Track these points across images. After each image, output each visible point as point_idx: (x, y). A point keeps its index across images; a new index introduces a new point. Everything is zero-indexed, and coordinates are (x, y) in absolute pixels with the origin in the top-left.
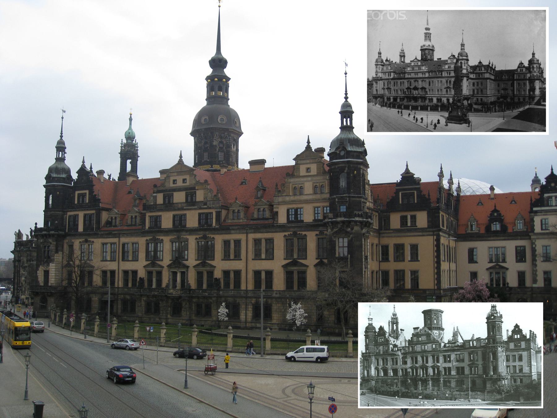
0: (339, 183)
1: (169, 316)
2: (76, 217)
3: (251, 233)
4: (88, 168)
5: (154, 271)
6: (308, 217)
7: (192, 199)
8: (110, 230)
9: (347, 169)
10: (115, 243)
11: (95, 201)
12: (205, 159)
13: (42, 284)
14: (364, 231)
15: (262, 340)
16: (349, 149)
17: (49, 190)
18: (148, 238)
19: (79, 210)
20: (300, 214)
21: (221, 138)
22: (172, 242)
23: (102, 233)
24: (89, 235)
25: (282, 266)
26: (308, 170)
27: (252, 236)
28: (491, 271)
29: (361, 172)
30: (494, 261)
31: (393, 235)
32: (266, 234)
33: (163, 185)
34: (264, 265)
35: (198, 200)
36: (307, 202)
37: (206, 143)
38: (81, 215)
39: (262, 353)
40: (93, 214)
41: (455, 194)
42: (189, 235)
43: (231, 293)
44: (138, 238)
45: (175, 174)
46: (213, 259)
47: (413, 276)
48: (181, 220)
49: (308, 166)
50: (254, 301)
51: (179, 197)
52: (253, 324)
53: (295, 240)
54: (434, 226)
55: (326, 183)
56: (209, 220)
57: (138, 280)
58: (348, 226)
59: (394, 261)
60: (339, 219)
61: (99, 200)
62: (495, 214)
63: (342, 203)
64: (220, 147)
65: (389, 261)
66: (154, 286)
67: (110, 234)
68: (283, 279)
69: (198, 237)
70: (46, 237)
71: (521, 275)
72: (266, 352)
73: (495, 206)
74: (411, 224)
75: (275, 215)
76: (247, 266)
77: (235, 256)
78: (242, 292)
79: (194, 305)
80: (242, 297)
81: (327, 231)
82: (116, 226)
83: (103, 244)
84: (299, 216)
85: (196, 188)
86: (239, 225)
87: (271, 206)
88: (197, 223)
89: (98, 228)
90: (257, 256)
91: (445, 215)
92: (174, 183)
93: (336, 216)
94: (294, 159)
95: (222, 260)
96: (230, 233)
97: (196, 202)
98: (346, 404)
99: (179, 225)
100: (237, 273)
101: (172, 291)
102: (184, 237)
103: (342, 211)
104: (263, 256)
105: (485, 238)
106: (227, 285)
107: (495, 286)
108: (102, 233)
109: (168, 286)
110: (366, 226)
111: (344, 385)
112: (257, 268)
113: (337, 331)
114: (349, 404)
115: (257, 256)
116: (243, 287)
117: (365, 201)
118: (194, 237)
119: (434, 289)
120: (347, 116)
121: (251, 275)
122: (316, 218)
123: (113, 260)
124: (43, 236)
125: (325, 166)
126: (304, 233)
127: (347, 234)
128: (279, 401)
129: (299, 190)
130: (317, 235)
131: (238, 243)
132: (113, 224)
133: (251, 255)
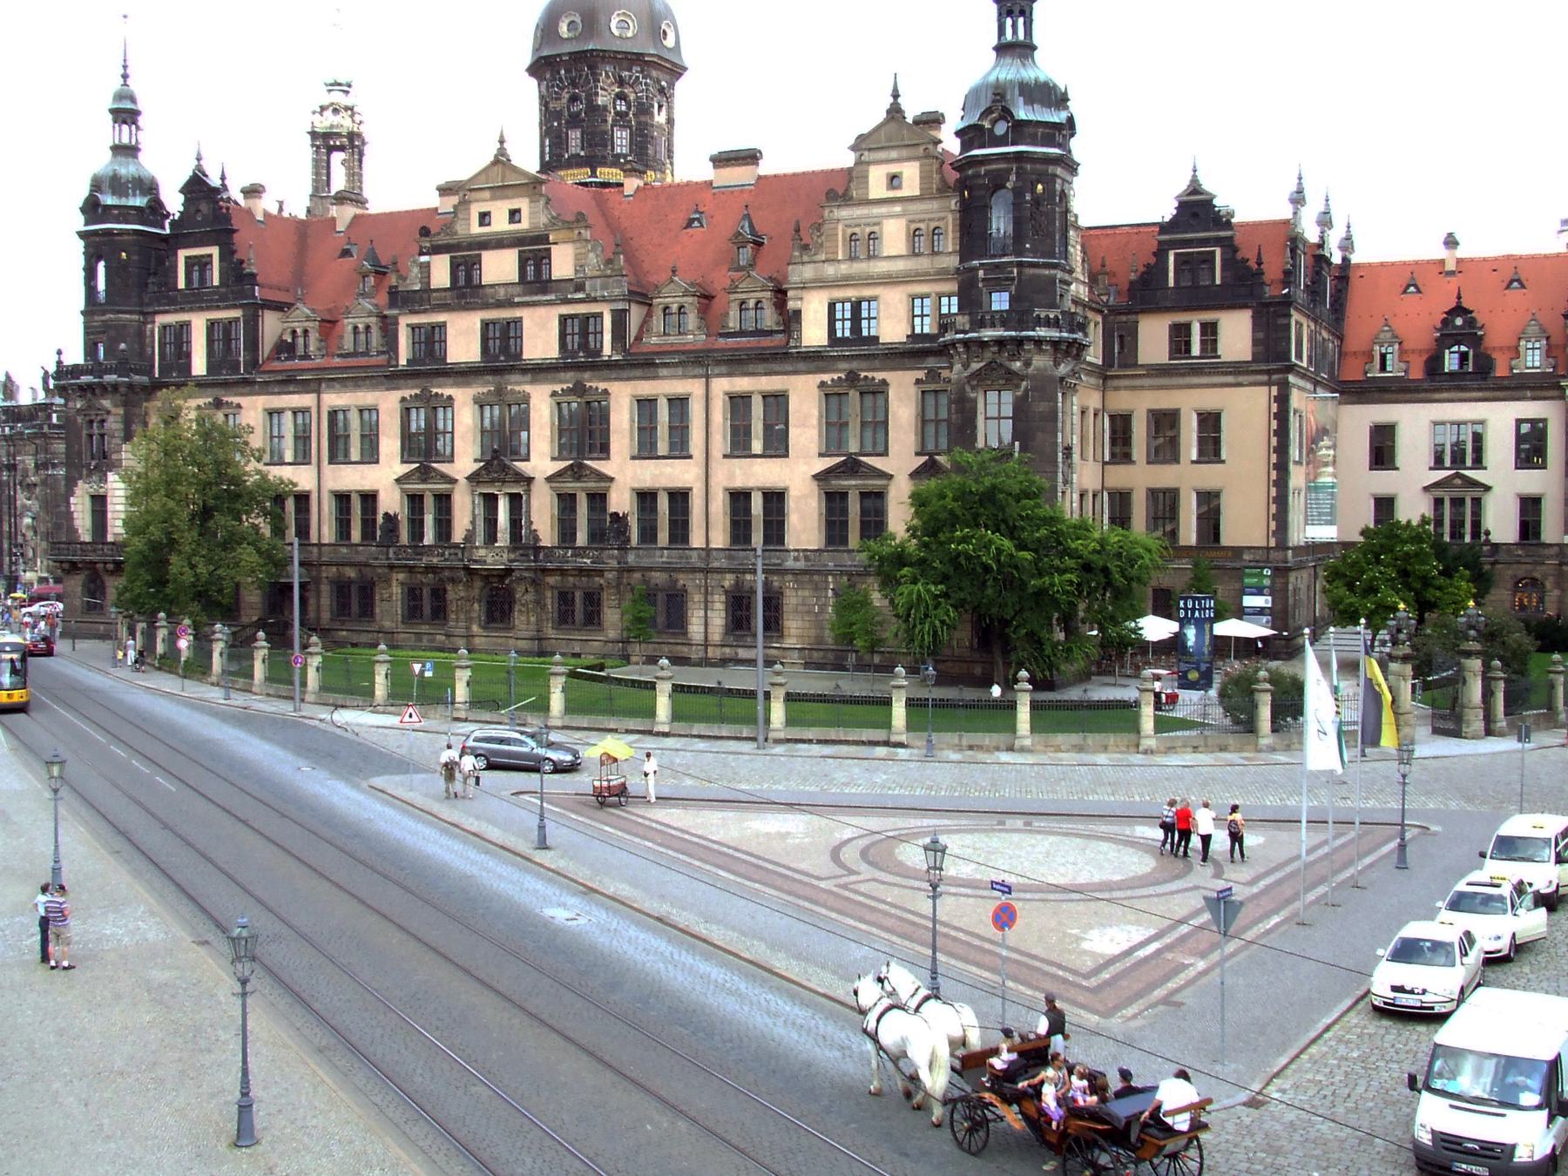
0: (986, 221)
1: (475, 628)
2: (181, 334)
4: (215, 181)
5: (428, 495)
6: (891, 326)
7: (538, 271)
8: (286, 370)
9: (1013, 177)
10: (305, 411)
11: (239, 279)
12: (573, 150)
13: (86, 537)
14: (1063, 369)
15: (761, 696)
16: (1022, 113)
17: (97, 247)
18: (407, 393)
19: (191, 310)
20: (869, 319)
21: (621, 82)
22: (480, 403)
23: (266, 378)
24: (226, 385)
25: (816, 477)
26: (894, 180)
27: (723, 385)
28: (1439, 493)
29: (1058, 187)
30: (1448, 463)
31: (1147, 382)
32: (764, 379)
33: (448, 227)
34: (759, 473)
35: (557, 273)
36: (890, 280)
37: (574, 99)
38: (199, 323)
39: (761, 738)
41: (1336, 259)
42: (533, 382)
43: (663, 558)
45: (487, 194)
46: (604, 450)
47: (1205, 508)
48: (505, 337)
49: (893, 168)
50: (729, 581)
51: (500, 267)
52: (727, 650)
53: (854, 395)
54: (1271, 358)
55: (950, 224)
56: (591, 337)
57: (380, 520)
58: (1013, 358)
59: (1149, 463)
60: (988, 334)
61: (253, 276)
62: (1459, 321)
63: (997, 284)
64: (617, 113)
65: (1133, 462)
66: (429, 538)
67: (289, 383)
68: (816, 516)
69: (558, 388)
70: (94, 394)
71: (1530, 506)
72: (772, 735)
73: (1459, 297)
74: (1203, 350)
75: (791, 320)
76: (708, 474)
77: (672, 446)
78: (694, 554)
79: (549, 594)
80: (694, 570)
81: (951, 368)
82: (306, 357)
83: (272, 413)
84: (864, 323)
86: (683, 352)
87: (780, 294)
88: (556, 346)
89: (253, 364)
90: (739, 446)
91: (1304, 321)
92: (481, 224)
93: (981, 324)
94: (853, 148)
95: (633, 458)
97: (550, 281)
98: (1028, 896)
99: (502, 352)
100: (680, 498)
101: (482, 552)
102: (517, 388)
103: (995, 307)
104: (757, 446)
105: (1422, 395)
106: (649, 534)
107: (1447, 538)
108: (266, 378)
109: (470, 536)
110: (1067, 353)
111: (1016, 837)
112: (739, 483)
113: (978, 670)
114: (1037, 896)
115: (739, 446)
116: (697, 540)
117: (1067, 277)
119: (1268, 548)
120: (1017, 10)
121: (719, 504)
122: (918, 330)
123: (303, 458)
124: (84, 389)
125: (947, 167)
126: (879, 376)
127: (1011, 379)
128: (823, 885)
129: (865, 244)
130: (918, 382)
131: (679, 404)
132: (300, 351)
133: (720, 443)
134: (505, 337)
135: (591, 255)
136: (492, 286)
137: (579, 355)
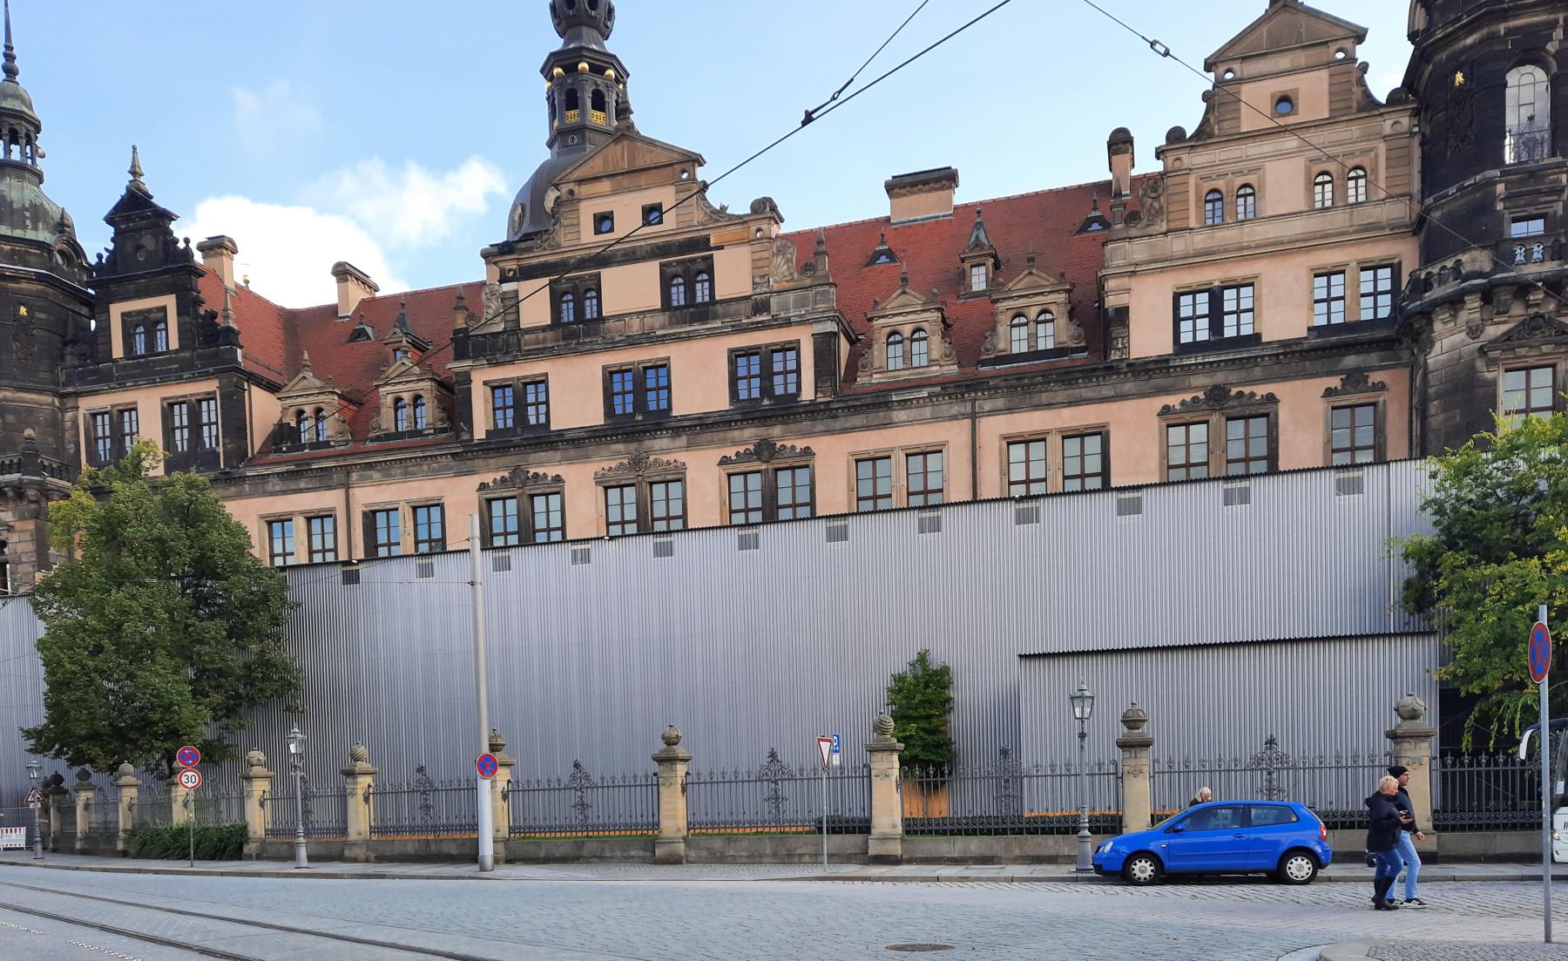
3: (992, 413)
7: (690, 293)
18: (488, 478)
19: (136, 386)
38: (148, 404)
40: (210, 397)
42: (689, 447)
44: (440, 483)
48: (640, 391)
51: (630, 290)
67: (300, 475)
84: (1229, 321)
85: (713, 242)
92: (598, 231)
96: (888, 424)
102: (665, 458)
118: (716, 454)
132: (305, 438)
134: (640, 391)
135: (779, 260)
136: (620, 317)
137: (762, 406)
